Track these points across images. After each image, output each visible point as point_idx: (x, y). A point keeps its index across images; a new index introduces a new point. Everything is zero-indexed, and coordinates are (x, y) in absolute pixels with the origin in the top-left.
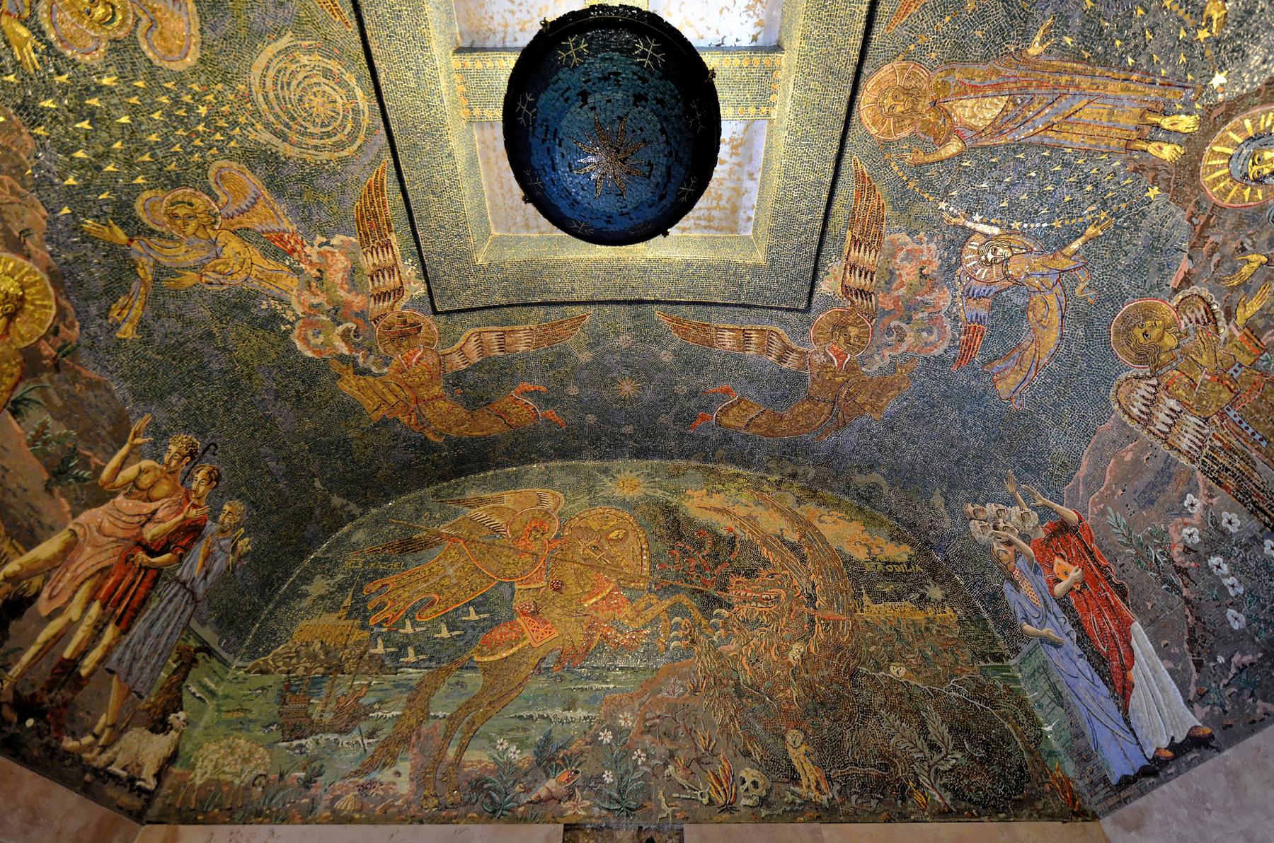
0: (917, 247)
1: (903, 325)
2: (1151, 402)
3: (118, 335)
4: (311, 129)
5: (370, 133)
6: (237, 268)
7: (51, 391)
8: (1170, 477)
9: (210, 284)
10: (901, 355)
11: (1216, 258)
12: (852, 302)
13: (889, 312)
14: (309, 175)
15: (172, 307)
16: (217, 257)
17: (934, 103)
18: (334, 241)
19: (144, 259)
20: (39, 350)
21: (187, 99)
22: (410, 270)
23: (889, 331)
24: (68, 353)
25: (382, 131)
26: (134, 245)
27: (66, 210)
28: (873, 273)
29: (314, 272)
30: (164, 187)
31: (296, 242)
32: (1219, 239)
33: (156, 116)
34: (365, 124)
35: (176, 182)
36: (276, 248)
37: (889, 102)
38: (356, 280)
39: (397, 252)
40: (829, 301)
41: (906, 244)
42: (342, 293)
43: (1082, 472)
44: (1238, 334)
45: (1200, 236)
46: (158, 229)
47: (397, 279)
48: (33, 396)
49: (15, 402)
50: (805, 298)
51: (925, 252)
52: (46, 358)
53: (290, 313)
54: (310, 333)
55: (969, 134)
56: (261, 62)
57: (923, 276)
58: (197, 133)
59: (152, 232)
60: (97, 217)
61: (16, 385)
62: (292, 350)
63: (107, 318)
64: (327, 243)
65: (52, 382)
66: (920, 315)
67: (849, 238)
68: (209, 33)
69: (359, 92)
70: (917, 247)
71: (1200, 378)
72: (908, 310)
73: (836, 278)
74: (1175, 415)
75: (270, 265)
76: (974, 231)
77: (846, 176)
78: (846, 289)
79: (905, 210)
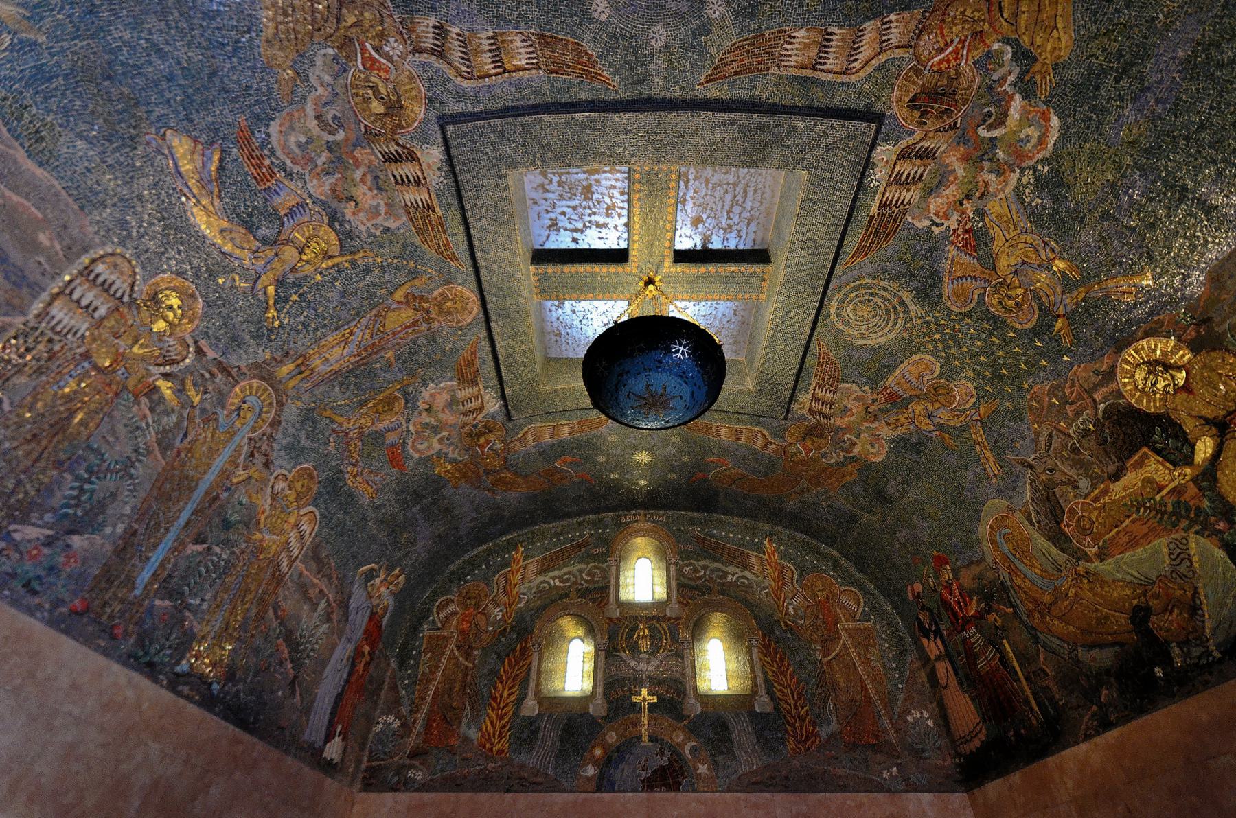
0: (375, 221)
1: (331, 138)
2: (106, 287)
4: (879, 301)
5: (840, 288)
6: (1020, 246)
8: (15, 283)
9: (1053, 250)
10: (304, 98)
11: (207, 375)
12: (398, 145)
13: (355, 146)
14: (906, 276)
16: (1024, 263)
17: (428, 312)
18: (927, 223)
19: (1068, 301)
21: (940, 345)
22: (879, 175)
23: (339, 122)
25: (831, 286)
28: (397, 183)
29: (967, 204)
30: (1003, 322)
31: (958, 236)
32: (217, 380)
33: (965, 349)
34: (842, 293)
35: (993, 319)
36: (976, 240)
37: (459, 306)
38: (936, 181)
39: (878, 196)
40: (423, 139)
41: (385, 220)
42: (961, 173)
43: (20, 155)
44: (151, 380)
45: (224, 369)
46: (1036, 307)
47: (897, 170)
50: (452, 141)
51: (364, 220)
52: (1198, 332)
53: (1025, 180)
54: (1029, 146)
55: (394, 306)
56: (883, 340)
57: (350, 199)
58: (953, 330)
59: (1040, 309)
62: (1064, 137)
64: (934, 223)
66: (323, 159)
67: (437, 209)
68: (899, 360)
69: (833, 311)
70: (375, 221)
71: (122, 343)
72: (339, 160)
73: (429, 166)
74: (89, 309)
75: (995, 231)
76: (341, 255)
77: (465, 256)
78: (412, 157)
79: (404, 246)
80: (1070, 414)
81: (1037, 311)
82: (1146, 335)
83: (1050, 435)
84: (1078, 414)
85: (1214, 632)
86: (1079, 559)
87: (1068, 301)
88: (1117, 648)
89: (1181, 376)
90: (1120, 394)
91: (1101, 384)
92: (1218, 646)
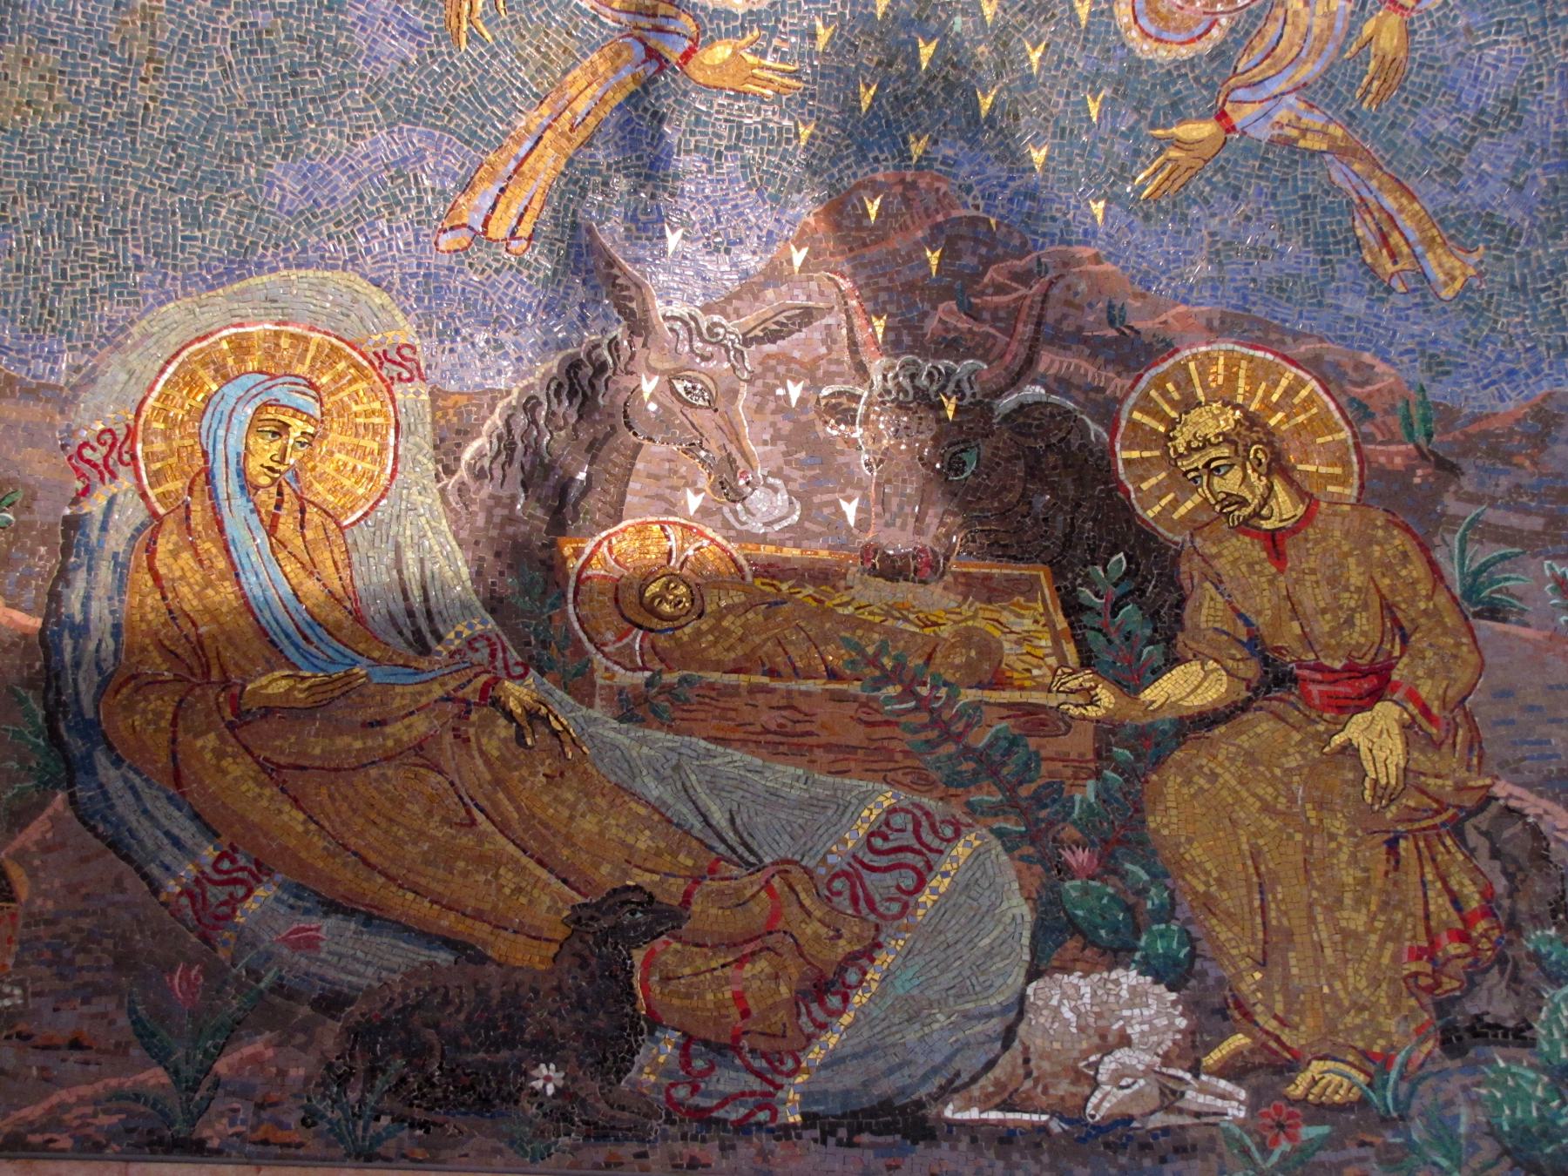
3: (1447, 294)
7: (1495, 516)
15: (1442, 126)
20: (1382, 473)
24: (1426, 420)
26: (1241, 116)
27: (1098, 208)
48: (1481, 554)
49: (1471, 592)
52: (1411, 470)
59: (1218, 53)
60: (1137, 153)
61: (1433, 566)
63: (1390, 290)
65: (1474, 499)
80: (932, 325)
81: (1205, 46)
82: (1312, 364)
83: (807, 316)
84: (951, 346)
85: (834, 1061)
86: (531, 663)
87: (1282, 115)
88: (444, 957)
89: (1285, 507)
90: (1108, 414)
91: (1096, 348)
92: (807, 1097)
